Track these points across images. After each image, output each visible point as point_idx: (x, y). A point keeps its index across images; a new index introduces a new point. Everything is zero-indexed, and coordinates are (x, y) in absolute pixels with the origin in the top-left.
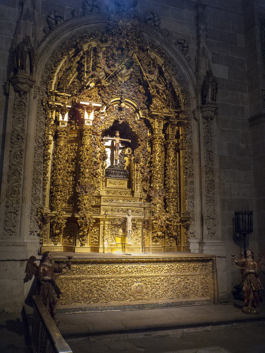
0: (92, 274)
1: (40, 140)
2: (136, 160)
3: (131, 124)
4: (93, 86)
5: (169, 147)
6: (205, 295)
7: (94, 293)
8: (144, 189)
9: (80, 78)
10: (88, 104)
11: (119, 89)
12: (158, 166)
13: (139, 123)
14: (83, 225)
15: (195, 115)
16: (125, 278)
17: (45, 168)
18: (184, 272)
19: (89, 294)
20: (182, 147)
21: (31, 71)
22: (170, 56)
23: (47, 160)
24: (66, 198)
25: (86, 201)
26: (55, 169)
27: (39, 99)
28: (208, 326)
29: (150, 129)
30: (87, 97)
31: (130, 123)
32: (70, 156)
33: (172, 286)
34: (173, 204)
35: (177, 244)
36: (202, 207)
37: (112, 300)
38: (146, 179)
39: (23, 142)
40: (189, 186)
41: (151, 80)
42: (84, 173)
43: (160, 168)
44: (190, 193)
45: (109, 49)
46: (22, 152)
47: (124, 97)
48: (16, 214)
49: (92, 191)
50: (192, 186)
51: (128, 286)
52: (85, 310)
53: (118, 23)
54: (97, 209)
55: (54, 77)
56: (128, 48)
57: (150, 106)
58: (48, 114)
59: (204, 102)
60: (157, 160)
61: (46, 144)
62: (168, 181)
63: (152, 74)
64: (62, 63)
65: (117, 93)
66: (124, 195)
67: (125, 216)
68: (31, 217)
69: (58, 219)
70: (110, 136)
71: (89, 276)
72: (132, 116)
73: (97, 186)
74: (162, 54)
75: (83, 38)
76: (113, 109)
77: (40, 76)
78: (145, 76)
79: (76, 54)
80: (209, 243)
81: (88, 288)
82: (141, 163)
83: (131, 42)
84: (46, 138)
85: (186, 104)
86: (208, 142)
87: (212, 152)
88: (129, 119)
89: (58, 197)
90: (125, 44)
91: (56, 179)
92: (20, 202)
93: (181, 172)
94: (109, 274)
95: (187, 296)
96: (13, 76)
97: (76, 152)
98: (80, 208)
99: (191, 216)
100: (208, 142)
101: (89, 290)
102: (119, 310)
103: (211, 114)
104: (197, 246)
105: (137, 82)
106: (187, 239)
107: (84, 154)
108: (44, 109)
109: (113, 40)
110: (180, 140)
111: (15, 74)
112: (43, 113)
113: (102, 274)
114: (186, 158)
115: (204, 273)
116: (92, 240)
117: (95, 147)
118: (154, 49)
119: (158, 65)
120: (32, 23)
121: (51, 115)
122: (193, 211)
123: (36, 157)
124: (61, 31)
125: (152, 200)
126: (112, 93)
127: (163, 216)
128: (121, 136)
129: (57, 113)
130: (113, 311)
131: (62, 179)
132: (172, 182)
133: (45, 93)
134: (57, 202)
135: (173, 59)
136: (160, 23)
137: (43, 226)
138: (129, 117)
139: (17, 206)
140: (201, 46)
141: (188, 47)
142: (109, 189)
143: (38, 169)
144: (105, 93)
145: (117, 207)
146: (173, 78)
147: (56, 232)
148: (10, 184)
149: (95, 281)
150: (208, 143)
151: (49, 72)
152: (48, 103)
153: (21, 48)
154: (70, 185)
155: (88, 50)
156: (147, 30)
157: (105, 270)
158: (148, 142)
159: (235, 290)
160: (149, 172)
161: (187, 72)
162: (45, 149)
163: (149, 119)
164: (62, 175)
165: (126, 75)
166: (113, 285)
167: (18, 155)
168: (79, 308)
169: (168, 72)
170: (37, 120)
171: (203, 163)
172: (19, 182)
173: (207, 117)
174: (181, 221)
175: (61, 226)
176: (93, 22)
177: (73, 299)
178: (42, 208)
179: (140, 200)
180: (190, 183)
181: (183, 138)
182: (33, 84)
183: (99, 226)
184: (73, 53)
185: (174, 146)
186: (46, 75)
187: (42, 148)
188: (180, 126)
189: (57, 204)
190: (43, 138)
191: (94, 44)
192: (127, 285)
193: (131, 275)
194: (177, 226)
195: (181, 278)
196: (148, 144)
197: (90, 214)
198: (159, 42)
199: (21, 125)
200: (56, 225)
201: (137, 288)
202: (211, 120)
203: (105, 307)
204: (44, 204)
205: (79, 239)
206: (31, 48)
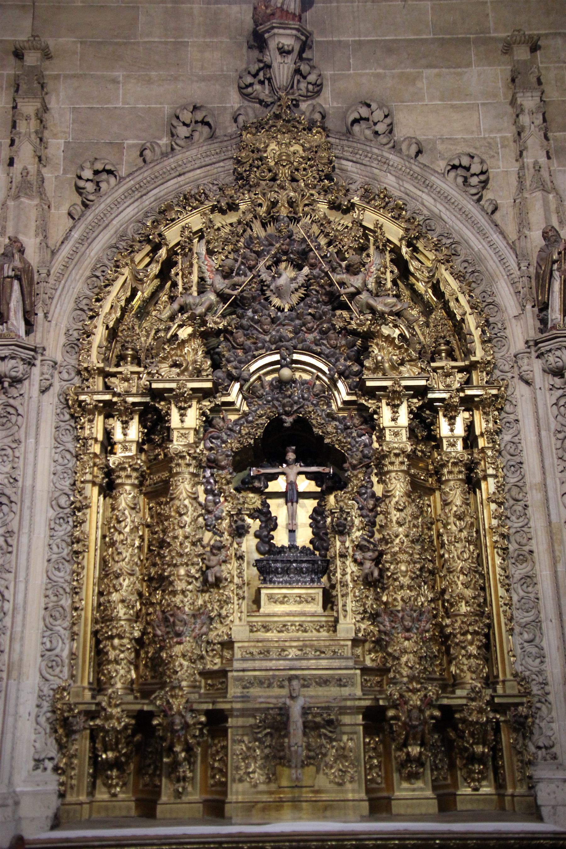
5: (443, 475)
12: (397, 536)
13: (344, 418)
15: (523, 369)
21: (30, 326)
26: (107, 575)
30: (171, 366)
31: (314, 422)
32: (156, 533)
34: (467, 651)
40: (520, 591)
41: (352, 289)
42: (172, 578)
43: (403, 543)
44: (526, 614)
46: (9, 540)
47: (287, 349)
53: (266, 151)
55: (96, 327)
58: (81, 428)
60: (394, 519)
65: (270, 341)
66: (315, 633)
70: (268, 461)
73: (224, 612)
77: (64, 331)
88: (310, 409)
89: (112, 655)
91: (109, 602)
105: (326, 304)
108: (72, 416)
110: (476, 451)
112: (69, 427)
119: (388, 241)
120: (36, 201)
123: (55, 547)
124: (112, 206)
126: (255, 343)
131: (123, 601)
132: (459, 583)
133: (73, 374)
135: (441, 218)
138: (312, 404)
140: (529, 160)
145: (277, 673)
163: (364, 402)
164: (124, 587)
170: (56, 448)
176: (196, 166)
180: (523, 581)
182: (33, 357)
184: (147, 255)
190: (70, 492)
198: (393, 179)
199: (8, 468)
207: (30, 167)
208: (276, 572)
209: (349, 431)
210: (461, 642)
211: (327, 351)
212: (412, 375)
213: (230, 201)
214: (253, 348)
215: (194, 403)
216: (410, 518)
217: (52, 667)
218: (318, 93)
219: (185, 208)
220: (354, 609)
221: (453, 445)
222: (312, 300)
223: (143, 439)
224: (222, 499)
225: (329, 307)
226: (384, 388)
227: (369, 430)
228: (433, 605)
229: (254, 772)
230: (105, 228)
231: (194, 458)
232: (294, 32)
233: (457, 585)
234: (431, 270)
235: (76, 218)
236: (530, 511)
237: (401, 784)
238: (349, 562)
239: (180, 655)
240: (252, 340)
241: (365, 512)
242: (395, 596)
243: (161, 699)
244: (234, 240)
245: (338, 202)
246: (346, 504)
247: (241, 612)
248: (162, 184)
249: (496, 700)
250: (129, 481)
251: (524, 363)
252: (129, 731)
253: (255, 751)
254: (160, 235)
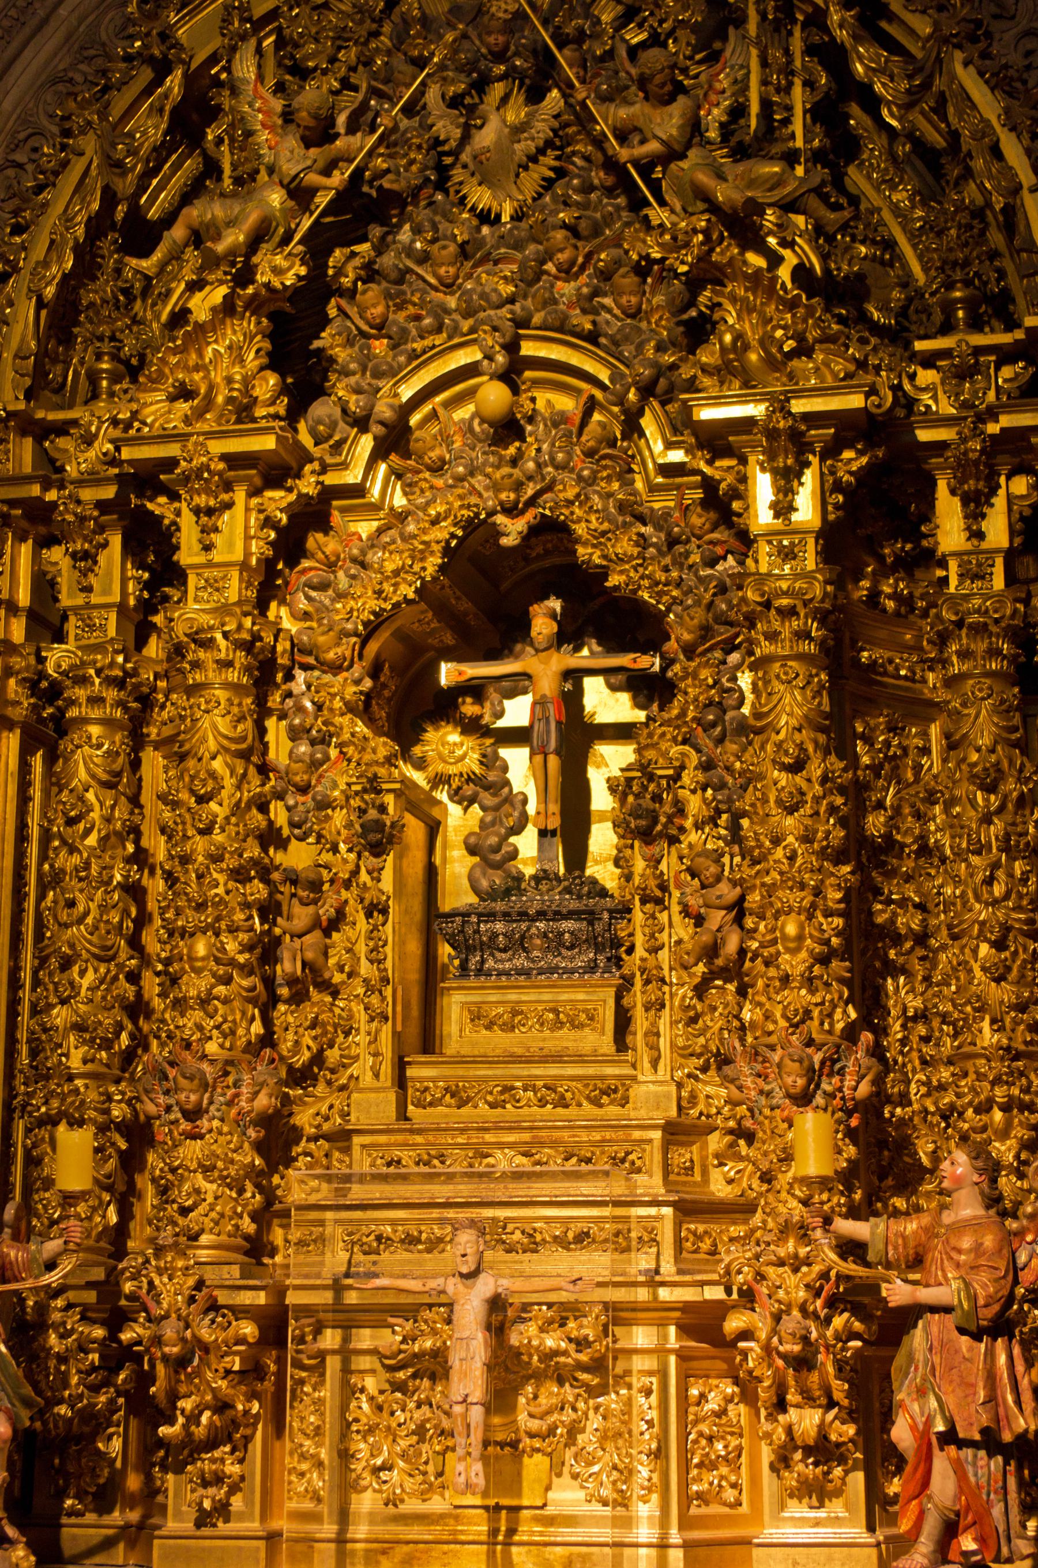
11: (469, 276)
12: (776, 841)
13: (667, 514)
14: (161, 1369)
30: (172, 399)
31: (580, 529)
43: (792, 858)
47: (495, 329)
49: (252, 1100)
72: (605, 467)
82: (694, 837)
91: (45, 1030)
105: (610, 192)
107: (184, 823)
126: (418, 318)
127: (796, 1270)
131: (79, 1027)
138: (580, 479)
146: (959, 69)
208: (491, 944)
209: (680, 549)
210: (973, 1129)
212: (830, 381)
214: (414, 332)
215: (240, 495)
216: (818, 789)
220: (680, 1042)
221: (975, 574)
222: (568, 185)
223: (139, 599)
224: (333, 753)
225: (621, 201)
226: (747, 424)
227: (734, 543)
228: (922, 1030)
229: (387, 1467)
230: (39, 28)
231: (248, 647)
233: (970, 971)
234: (921, 69)
237: (782, 1507)
239: (194, 1165)
240: (411, 310)
243: (133, 1278)
244: (362, 32)
246: (665, 754)
247: (376, 1055)
250: (96, 713)
252: (94, 1357)
253: (392, 1414)
254: (165, 36)
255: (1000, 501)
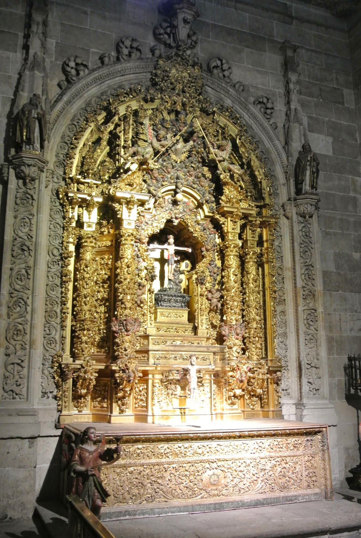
0: (144, 458)
1: (56, 252)
2: (201, 280)
3: (192, 226)
4: (136, 169)
5: (247, 258)
6: (312, 486)
7: (147, 488)
8: (212, 324)
9: (112, 155)
10: (128, 196)
12: (233, 288)
13: (204, 224)
14: (125, 382)
16: (192, 464)
17: (64, 295)
18: (280, 451)
19: (139, 489)
20: (268, 259)
22: (247, 123)
23: (67, 283)
24: (94, 339)
25: (127, 345)
26: (78, 296)
27: (54, 189)
28: (324, 535)
29: (219, 233)
31: (189, 224)
32: (100, 274)
33: (263, 473)
35: (262, 407)
36: (299, 349)
37: (174, 497)
38: (215, 308)
39: (30, 255)
40: (279, 318)
41: (221, 159)
42: (124, 301)
45: (157, 112)
46: (29, 271)
47: (182, 184)
48: (21, 366)
50: (283, 318)
51: (198, 475)
52: (135, 515)
54: (144, 355)
55: (75, 154)
56: (185, 110)
57: (220, 199)
59: (299, 191)
60: (232, 279)
61: (64, 257)
62: (247, 311)
63: (223, 151)
64: (87, 134)
65: (170, 178)
66: (183, 333)
67: (185, 367)
68: (43, 370)
69: (85, 372)
71: (139, 461)
74: (235, 119)
75: (118, 96)
76: (165, 202)
77: (54, 154)
78: (212, 154)
79: (107, 121)
80: (311, 405)
81: (137, 481)
82: (208, 285)
83: (189, 101)
84: (65, 248)
85: (271, 195)
86: (307, 251)
87: (313, 267)
88: (188, 217)
89: (84, 339)
90: (181, 104)
91: (81, 310)
92: (27, 347)
93: (267, 297)
94: (168, 457)
95: (285, 488)
96: (15, 155)
97: (109, 269)
98: (118, 355)
99: (283, 363)
100: (307, 251)
101: (139, 483)
102: (186, 513)
103: (310, 209)
104: (293, 409)
105: (199, 162)
106: (278, 399)
107: (124, 272)
108: (61, 204)
109: (162, 99)
110: (263, 248)
111: (17, 152)
112: (58, 210)
113: (158, 457)
114: (273, 276)
115: (309, 452)
116: (136, 404)
117: (138, 261)
118: (224, 111)
119: (231, 135)
120: (42, 75)
121: (72, 213)
122: (286, 356)
123: (50, 277)
124: (85, 86)
125: (226, 340)
126: (163, 178)
128: (176, 244)
129: (81, 209)
130: (176, 514)
131: (90, 311)
132: (254, 313)
133: (61, 179)
134: (82, 345)
135: (251, 127)
136: (230, 73)
137: (62, 384)
139: (23, 353)
140: (293, 107)
141: (272, 108)
142: (159, 324)
143: (53, 296)
144: (151, 178)
145: (174, 353)
146: (252, 155)
147: (81, 393)
148: (11, 320)
149: (149, 468)
150: (306, 253)
151: (67, 148)
152: (66, 195)
153: (27, 112)
154: (101, 319)
155: (125, 114)
156: (212, 84)
157: (162, 451)
158: (217, 252)
159: (351, 475)
160: (220, 297)
161: (272, 146)
162: (63, 266)
163: (218, 217)
165: (183, 151)
166: (176, 474)
167: (23, 275)
168: (126, 511)
169: (245, 146)
170: (51, 221)
171: (300, 283)
172: (25, 317)
173: (304, 213)
174: (269, 372)
175: (90, 383)
176: (132, 72)
177: (116, 497)
178: (60, 356)
179: (207, 341)
180: (281, 314)
181: (269, 246)
183: (146, 382)
184: (103, 118)
185: (255, 258)
186: (63, 153)
187: (58, 264)
188: (265, 228)
189: (82, 349)
190: (60, 248)
191: (134, 105)
192: (197, 474)
193: (201, 458)
194: (263, 380)
195: (276, 460)
196: (217, 255)
197: (135, 365)
199: (27, 230)
200: (82, 383)
201: (211, 477)
202: (309, 217)
203: (164, 508)
204: (63, 349)
205: (117, 402)
206: (41, 112)
207: (39, 53)
209: (205, 231)
211: (199, 188)
213: (153, 97)
214: (161, 180)
215: (136, 206)
217: (50, 344)
218: (194, 47)
219: (129, 96)
224: (141, 260)
226: (232, 213)
227: (216, 232)
230: (80, 97)
232: (193, 13)
235: (64, 88)
236: (285, 280)
238: (204, 298)
239: (128, 341)
240: (162, 176)
241: (212, 274)
242: (232, 317)
245: (207, 109)
248: (113, 78)
249: (271, 369)
251: (288, 208)
255: (257, 232)
